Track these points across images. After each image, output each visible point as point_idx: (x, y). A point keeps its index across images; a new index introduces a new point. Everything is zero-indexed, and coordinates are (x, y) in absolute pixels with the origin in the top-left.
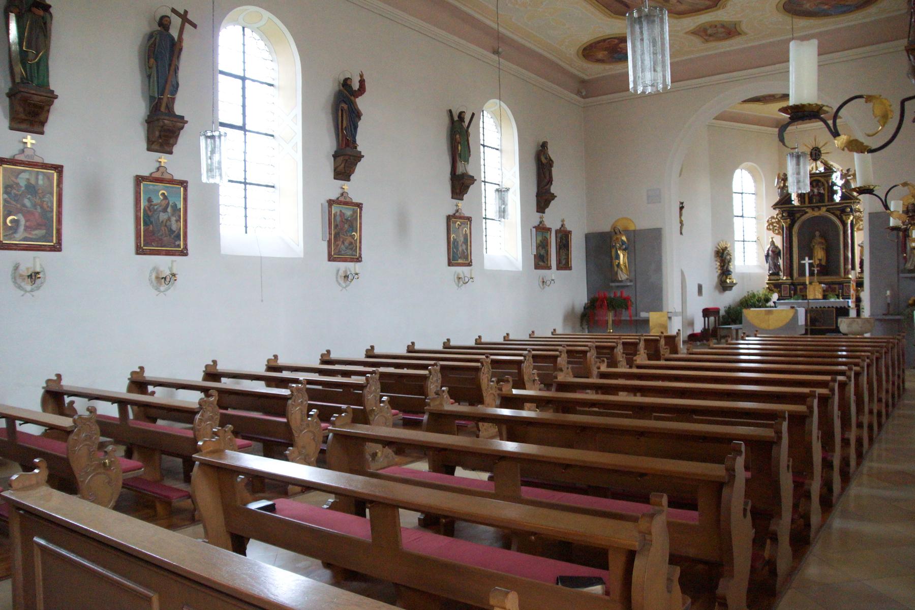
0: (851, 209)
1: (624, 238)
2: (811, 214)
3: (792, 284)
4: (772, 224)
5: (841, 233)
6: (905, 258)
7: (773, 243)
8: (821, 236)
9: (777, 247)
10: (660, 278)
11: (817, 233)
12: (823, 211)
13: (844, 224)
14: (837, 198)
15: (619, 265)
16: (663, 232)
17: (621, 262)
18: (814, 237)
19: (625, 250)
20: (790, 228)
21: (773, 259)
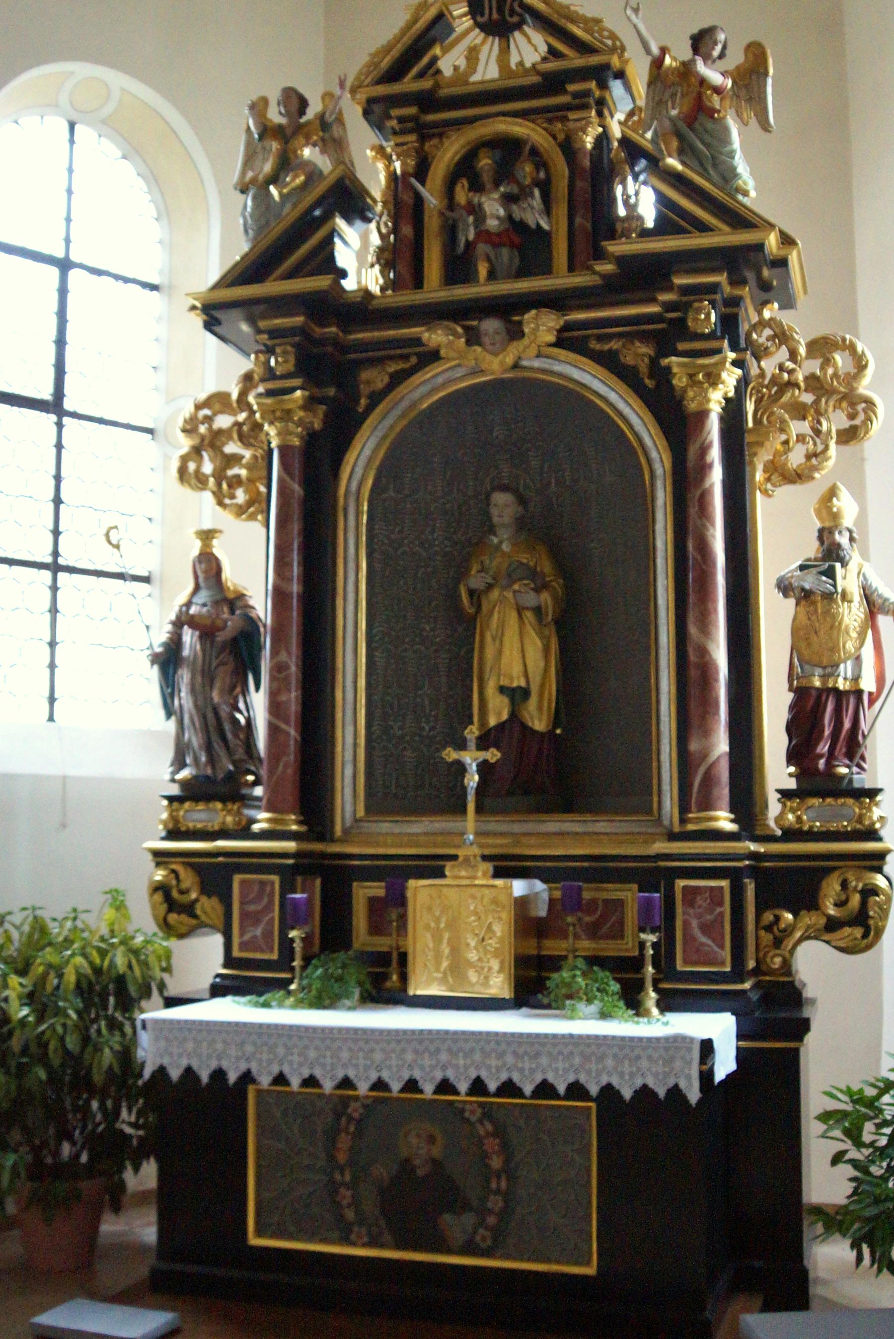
0: (729, 324)
2: (461, 363)
3: (297, 870)
4: (213, 441)
5: (662, 497)
7: (209, 568)
9: (235, 602)
11: (503, 506)
13: (678, 423)
20: (315, 466)
21: (206, 676)
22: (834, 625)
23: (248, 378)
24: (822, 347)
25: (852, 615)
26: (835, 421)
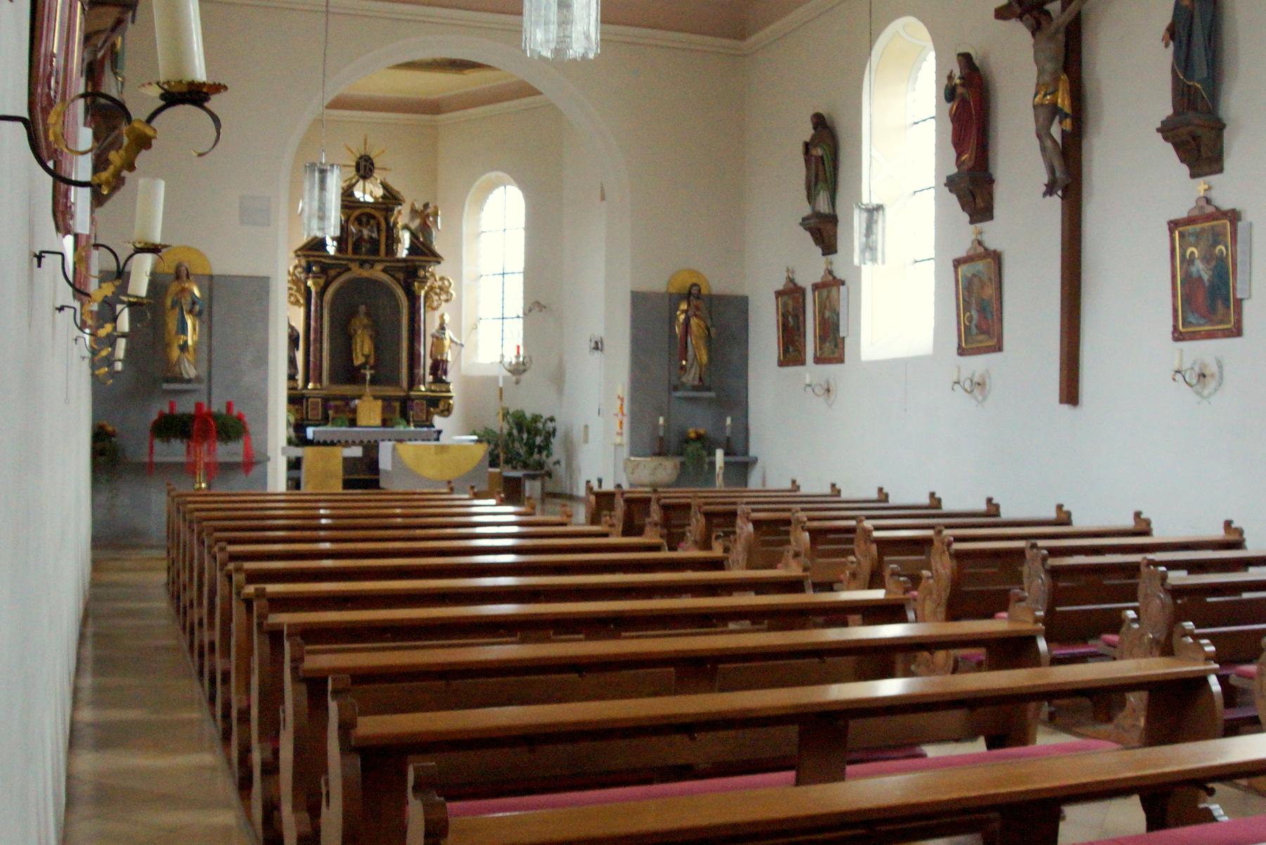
1: (197, 292)
2: (357, 271)
6: (683, 368)
8: (368, 314)
10: (265, 379)
11: (362, 308)
12: (377, 272)
13: (413, 298)
14: (403, 253)
15: (184, 347)
16: (272, 283)
17: (190, 342)
18: (353, 314)
19: (198, 315)
20: (321, 294)
22: (443, 345)
23: (296, 267)
24: (442, 279)
25: (447, 342)
26: (443, 297)
